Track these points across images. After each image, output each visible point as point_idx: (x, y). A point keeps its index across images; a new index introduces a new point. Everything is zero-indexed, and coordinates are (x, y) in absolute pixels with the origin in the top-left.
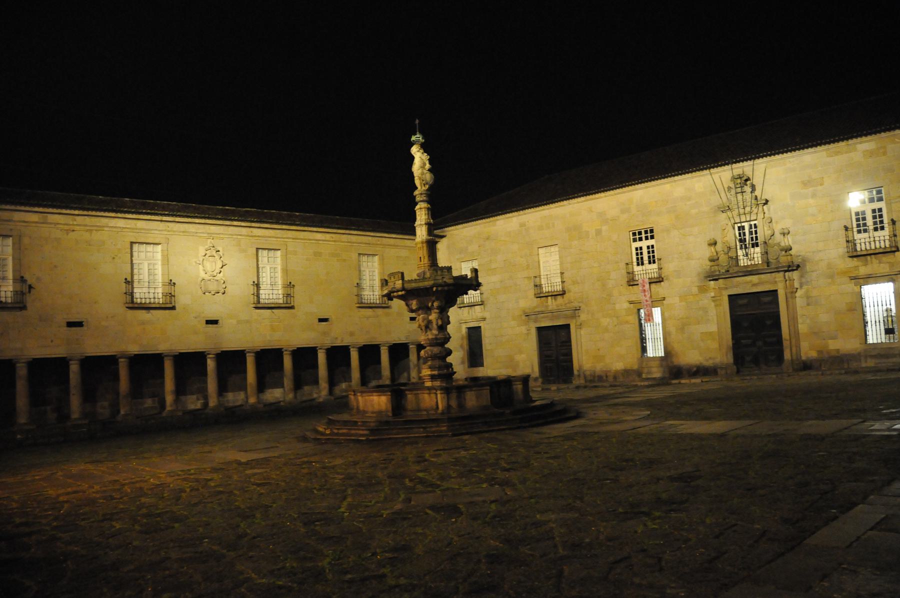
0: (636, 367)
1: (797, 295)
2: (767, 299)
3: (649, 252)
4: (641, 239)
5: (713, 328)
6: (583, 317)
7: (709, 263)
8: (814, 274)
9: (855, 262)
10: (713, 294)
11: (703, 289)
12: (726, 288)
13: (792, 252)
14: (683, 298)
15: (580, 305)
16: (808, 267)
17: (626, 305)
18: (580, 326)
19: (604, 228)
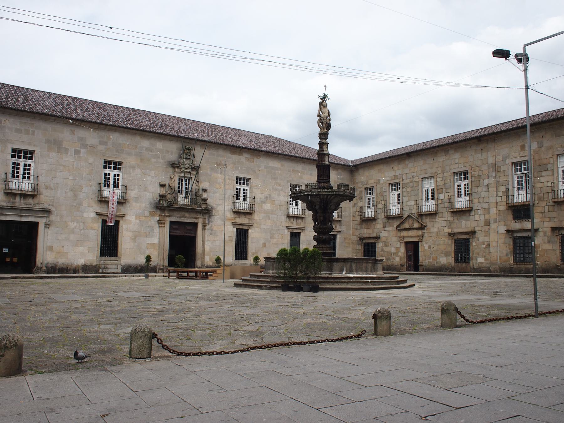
0: (94, 264)
1: (206, 228)
2: (190, 228)
3: (115, 179)
4: (110, 168)
5: (156, 241)
6: (53, 218)
7: (158, 197)
8: (216, 217)
9: (236, 216)
10: (158, 218)
11: (152, 214)
12: (170, 216)
13: (208, 202)
14: (138, 217)
15: (50, 207)
16: (214, 212)
17: (93, 215)
18: (47, 226)
19: (83, 151)
